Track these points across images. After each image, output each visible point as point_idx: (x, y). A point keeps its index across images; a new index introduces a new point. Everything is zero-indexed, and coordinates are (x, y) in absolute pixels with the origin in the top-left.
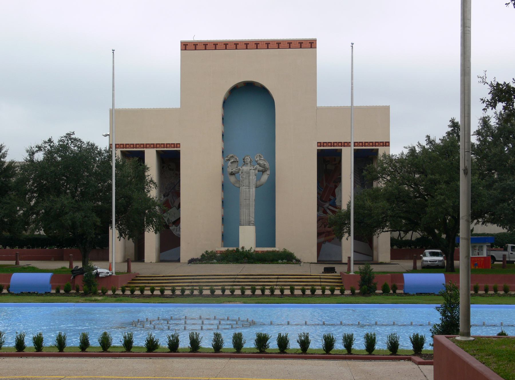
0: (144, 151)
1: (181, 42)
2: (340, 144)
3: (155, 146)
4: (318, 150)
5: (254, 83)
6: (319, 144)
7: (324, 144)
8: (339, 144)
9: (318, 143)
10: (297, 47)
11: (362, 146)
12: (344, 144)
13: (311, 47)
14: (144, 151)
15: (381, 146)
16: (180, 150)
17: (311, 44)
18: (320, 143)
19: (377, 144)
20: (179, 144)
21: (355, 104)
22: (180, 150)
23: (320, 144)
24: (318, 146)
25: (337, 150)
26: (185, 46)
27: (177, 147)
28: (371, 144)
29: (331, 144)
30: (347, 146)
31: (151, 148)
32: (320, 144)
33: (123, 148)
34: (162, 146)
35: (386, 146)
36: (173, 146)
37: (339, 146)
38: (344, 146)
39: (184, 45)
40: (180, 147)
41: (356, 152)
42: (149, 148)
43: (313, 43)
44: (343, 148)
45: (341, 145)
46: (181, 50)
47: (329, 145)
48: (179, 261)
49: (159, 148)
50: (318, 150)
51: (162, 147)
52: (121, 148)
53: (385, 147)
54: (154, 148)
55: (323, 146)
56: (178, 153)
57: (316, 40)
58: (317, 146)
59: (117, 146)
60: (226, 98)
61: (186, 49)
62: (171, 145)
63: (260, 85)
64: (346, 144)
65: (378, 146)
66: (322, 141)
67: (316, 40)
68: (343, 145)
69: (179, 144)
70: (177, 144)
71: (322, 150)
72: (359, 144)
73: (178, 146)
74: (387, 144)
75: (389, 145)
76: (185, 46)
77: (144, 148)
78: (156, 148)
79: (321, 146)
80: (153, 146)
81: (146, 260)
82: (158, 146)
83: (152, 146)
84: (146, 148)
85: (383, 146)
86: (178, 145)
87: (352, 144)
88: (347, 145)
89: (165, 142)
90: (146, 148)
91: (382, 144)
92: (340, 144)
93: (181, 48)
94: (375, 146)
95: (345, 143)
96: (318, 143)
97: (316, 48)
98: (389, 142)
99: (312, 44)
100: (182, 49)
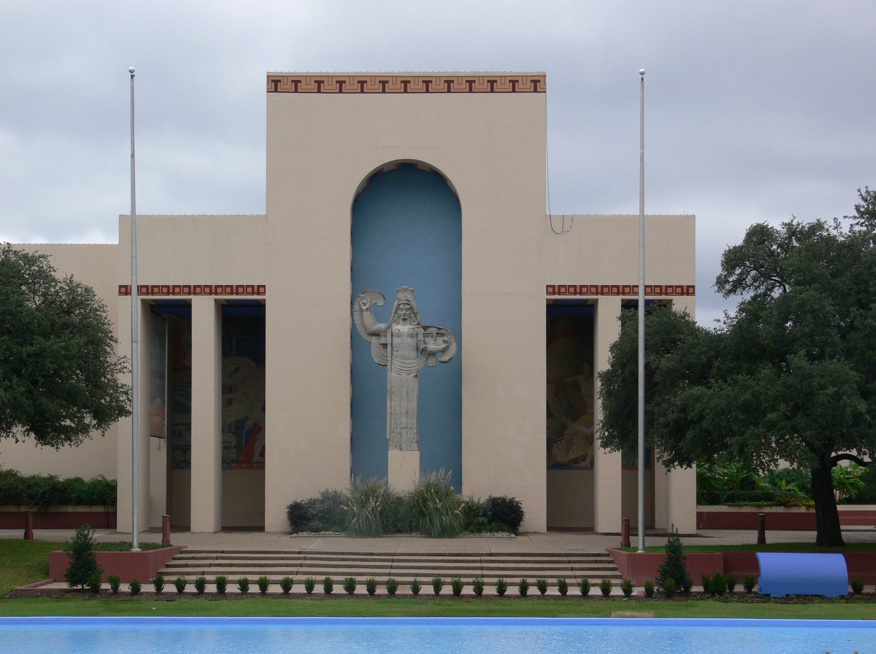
0: (191, 300)
3: (150, 291)
4: (548, 300)
5: (417, 164)
6: (550, 290)
9: (548, 286)
10: (484, 91)
12: (174, 290)
13: (535, 91)
14: (191, 300)
15: (677, 294)
16: (265, 300)
17: (491, 84)
18: (553, 286)
19: (670, 290)
20: (264, 286)
22: (265, 300)
25: (587, 300)
27: (258, 293)
31: (205, 294)
32: (552, 289)
33: (147, 294)
34: (228, 290)
35: (688, 294)
37: (592, 294)
38: (602, 294)
40: (265, 293)
42: (200, 294)
43: (539, 81)
44: (599, 297)
46: (267, 92)
48: (261, 529)
49: (221, 293)
50: (548, 300)
51: (227, 293)
53: (685, 297)
54: (211, 294)
55: (559, 293)
56: (260, 306)
58: (547, 292)
60: (360, 191)
62: (245, 289)
63: (430, 168)
65: (672, 294)
66: (557, 283)
67: (545, 76)
69: (264, 286)
70: (259, 287)
71: (556, 301)
73: (261, 290)
74: (691, 290)
75: (693, 294)
77: (190, 294)
78: (216, 294)
79: (554, 293)
81: (194, 527)
82: (219, 290)
83: (207, 290)
85: (682, 294)
86: (260, 289)
87: (134, 291)
90: (195, 295)
91: (679, 290)
93: (267, 89)
94: (666, 294)
95: (604, 288)
96: (548, 286)
97: (545, 92)
98: (693, 287)
99: (537, 84)
100: (269, 90)
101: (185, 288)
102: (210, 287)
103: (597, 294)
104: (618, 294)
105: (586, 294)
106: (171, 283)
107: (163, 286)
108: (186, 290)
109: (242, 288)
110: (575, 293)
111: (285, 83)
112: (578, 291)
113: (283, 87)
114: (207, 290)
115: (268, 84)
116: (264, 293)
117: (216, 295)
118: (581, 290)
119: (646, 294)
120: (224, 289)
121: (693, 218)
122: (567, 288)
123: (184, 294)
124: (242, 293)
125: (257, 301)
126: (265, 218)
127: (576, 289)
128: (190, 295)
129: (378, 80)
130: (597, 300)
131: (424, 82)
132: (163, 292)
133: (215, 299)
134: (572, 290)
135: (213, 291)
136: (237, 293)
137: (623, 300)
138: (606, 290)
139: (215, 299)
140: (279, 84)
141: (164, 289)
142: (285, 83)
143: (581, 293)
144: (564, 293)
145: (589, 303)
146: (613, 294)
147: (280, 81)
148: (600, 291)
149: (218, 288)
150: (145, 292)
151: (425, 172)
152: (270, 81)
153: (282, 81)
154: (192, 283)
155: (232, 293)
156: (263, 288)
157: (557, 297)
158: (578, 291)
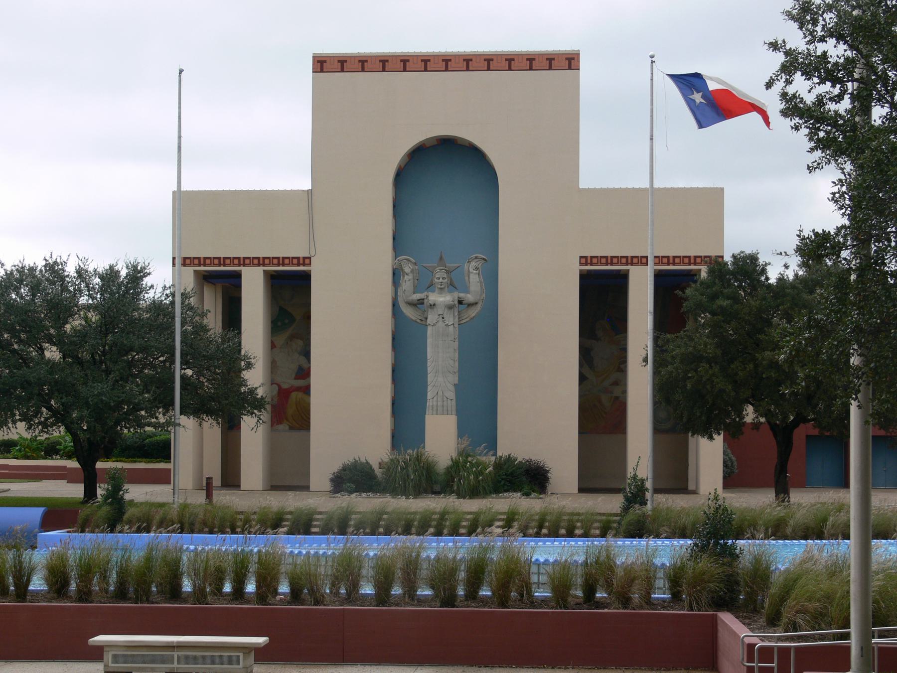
1: (314, 57)
4: (580, 271)
6: (583, 261)
7: (634, 259)
8: (685, 259)
13: (570, 68)
18: (586, 257)
21: (656, 186)
24: (581, 264)
25: (619, 271)
26: (321, 64)
27: (304, 265)
31: (254, 265)
32: (584, 260)
33: (199, 265)
37: (622, 264)
39: (318, 62)
40: (310, 264)
42: (249, 265)
43: (573, 59)
45: (688, 262)
46: (313, 72)
47: (602, 262)
49: (269, 265)
51: (274, 265)
52: (195, 265)
54: (259, 265)
55: (591, 264)
56: (305, 278)
57: (578, 55)
58: (580, 263)
59: (188, 262)
60: (403, 166)
61: (322, 71)
62: (292, 260)
63: (469, 144)
70: (304, 258)
71: (589, 271)
73: (307, 261)
76: (321, 64)
77: (239, 265)
78: (264, 265)
79: (586, 264)
80: (259, 262)
83: (256, 262)
84: (244, 265)
86: (306, 261)
88: (679, 262)
93: (313, 69)
94: (695, 264)
96: (581, 257)
97: (579, 69)
99: (571, 61)
106: (222, 255)
107: (273, 258)
108: (236, 262)
110: (668, 264)
112: (692, 261)
114: (256, 262)
116: (310, 264)
117: (263, 266)
119: (655, 264)
120: (271, 260)
121: (722, 189)
122: (600, 259)
123: (234, 265)
124: (288, 265)
125: (304, 271)
126: (309, 193)
127: (610, 260)
128: (239, 266)
132: (235, 263)
134: (686, 260)
138: (635, 261)
141: (274, 260)
144: (679, 264)
145: (621, 273)
148: (629, 262)
150: (237, 263)
151: (465, 146)
154: (242, 255)
156: (309, 260)
157: (589, 267)
158: (671, 261)
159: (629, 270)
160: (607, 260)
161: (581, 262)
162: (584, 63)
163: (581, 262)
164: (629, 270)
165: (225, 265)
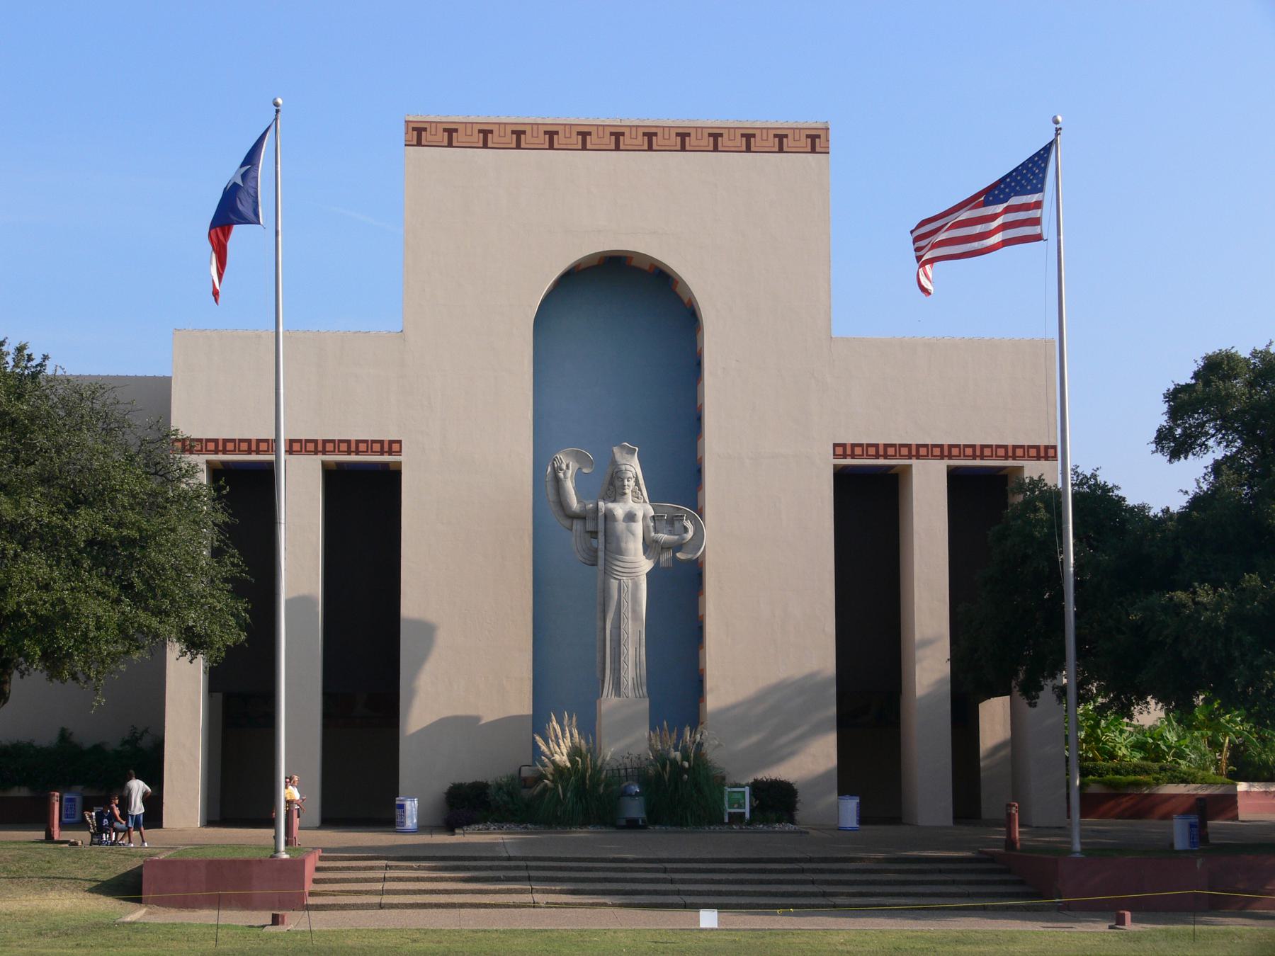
2: (905, 451)
4: (835, 466)
6: (839, 451)
9: (835, 445)
11: (974, 457)
15: (1030, 458)
18: (844, 446)
19: (1019, 452)
20: (399, 442)
23: (841, 448)
24: (836, 455)
27: (390, 453)
28: (969, 451)
29: (910, 451)
30: (895, 456)
31: (308, 452)
32: (841, 449)
33: (216, 452)
36: (377, 447)
37: (902, 457)
38: (918, 457)
39: (414, 129)
40: (400, 452)
41: (956, 479)
44: (914, 462)
49: (332, 452)
50: (835, 466)
52: (208, 452)
54: (316, 452)
55: (853, 456)
58: (834, 454)
64: (923, 451)
65: (1022, 458)
66: (849, 439)
68: (1042, 454)
69: (399, 442)
70: (391, 442)
71: (846, 467)
72: (932, 450)
73: (395, 447)
78: (324, 452)
79: (845, 456)
82: (329, 447)
83: (311, 447)
86: (393, 446)
89: (353, 436)
91: (1033, 452)
92: (905, 451)
94: (1014, 458)
96: (835, 445)
101: (242, 444)
102: (315, 442)
103: (910, 457)
104: (942, 457)
105: (894, 457)
107: (374, 442)
109: (332, 445)
111: (433, 132)
113: (430, 138)
114: (311, 447)
115: (407, 133)
116: (399, 452)
118: (853, 451)
122: (865, 449)
125: (385, 465)
129: (575, 130)
130: (908, 468)
131: (644, 134)
133: (323, 462)
135: (320, 448)
136: (357, 452)
137: (948, 467)
138: (923, 451)
139: (323, 462)
140: (424, 133)
142: (433, 132)
143: (886, 456)
146: (934, 457)
147: (425, 129)
149: (327, 444)
152: (410, 129)
153: (428, 130)
155: (349, 453)
159: (911, 465)
160: (1038, 452)
161: (837, 453)
162: (835, 140)
163: (837, 453)
164: (911, 465)
165: (258, 452)
